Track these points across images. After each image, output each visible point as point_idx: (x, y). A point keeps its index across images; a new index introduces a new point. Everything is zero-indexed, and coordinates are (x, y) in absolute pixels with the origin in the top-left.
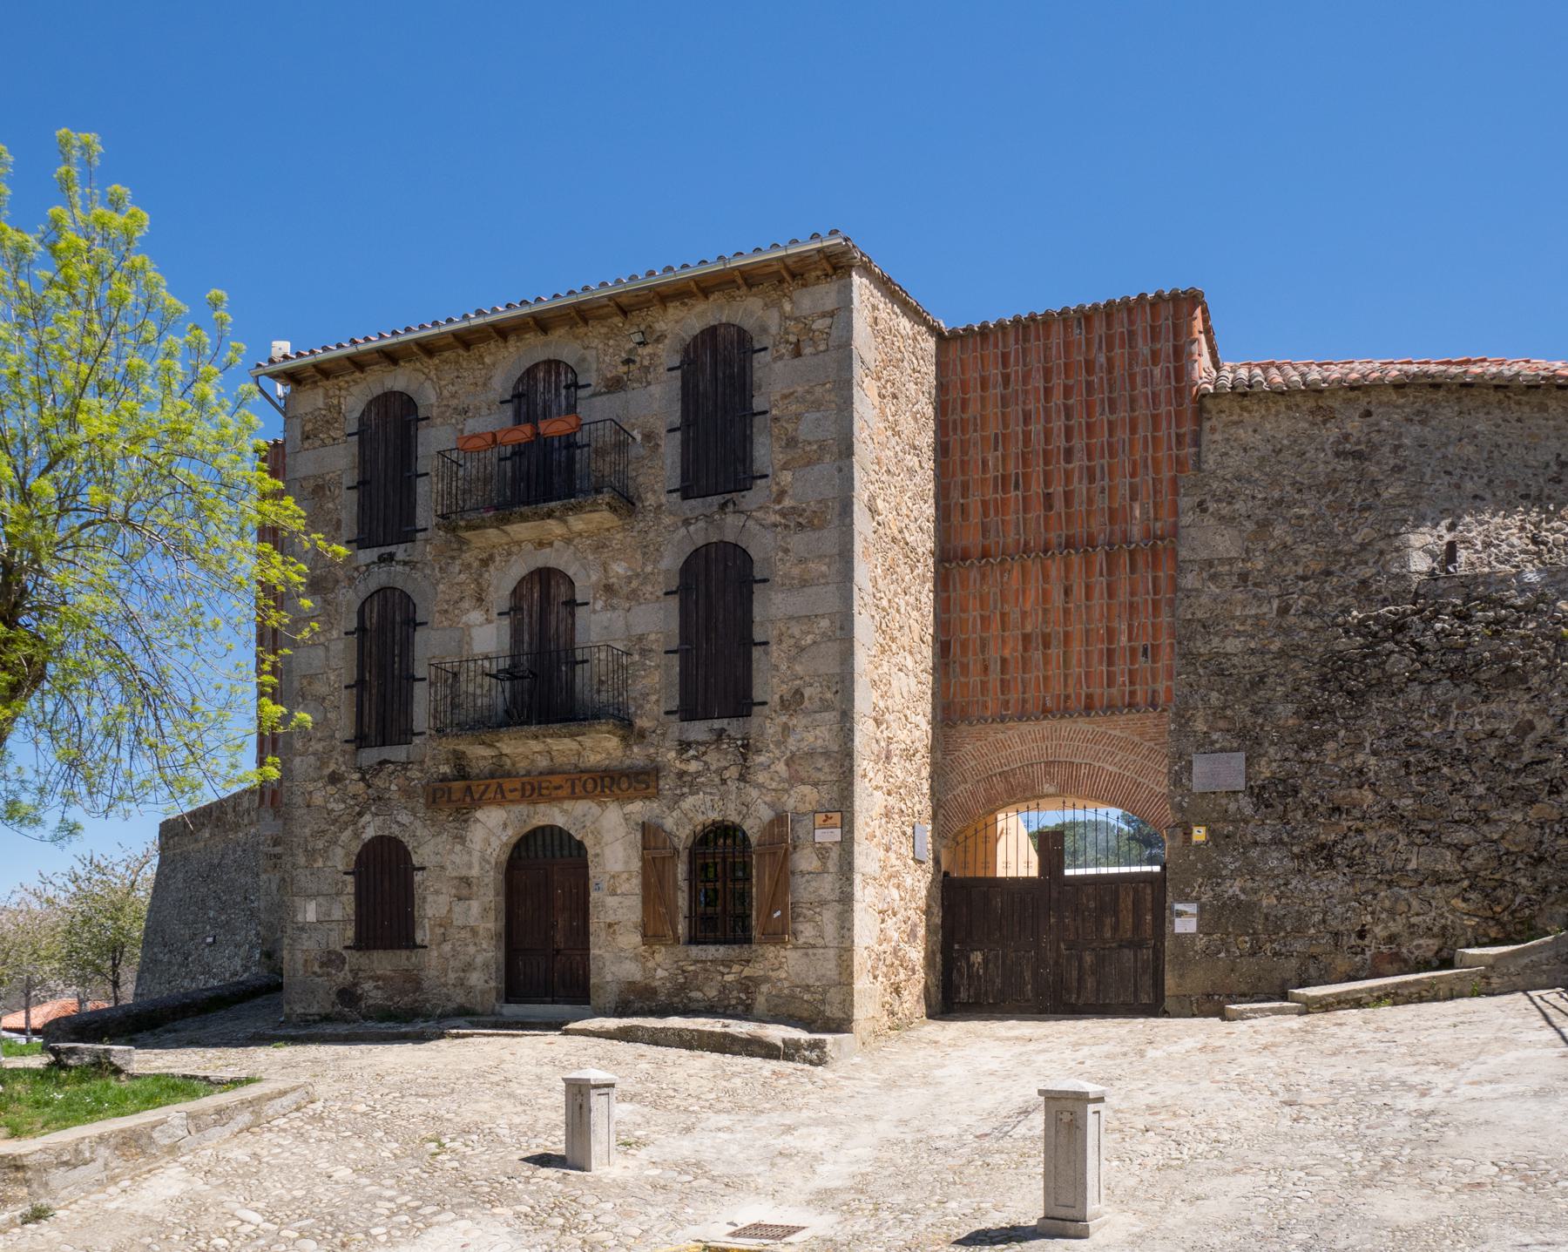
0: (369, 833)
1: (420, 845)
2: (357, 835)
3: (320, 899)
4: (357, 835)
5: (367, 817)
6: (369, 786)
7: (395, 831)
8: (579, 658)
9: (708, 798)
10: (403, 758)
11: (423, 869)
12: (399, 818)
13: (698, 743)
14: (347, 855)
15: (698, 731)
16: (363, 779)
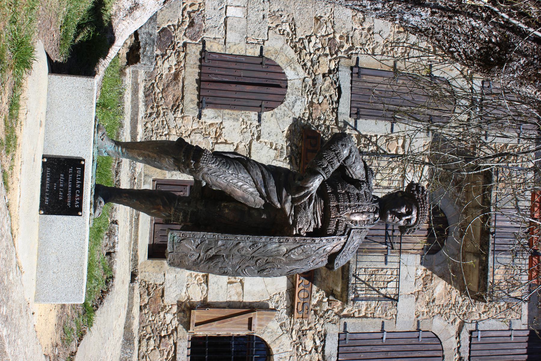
0: (290, 74)
1: (278, 119)
2: (290, 62)
3: (244, 21)
4: (290, 62)
5: (302, 74)
6: (324, 75)
7: (290, 99)
8: (389, 259)
9: (288, 355)
10: (341, 110)
11: (259, 120)
12: (299, 103)
13: (324, 347)
14: (276, 52)
15: (331, 347)
16: (330, 72)
